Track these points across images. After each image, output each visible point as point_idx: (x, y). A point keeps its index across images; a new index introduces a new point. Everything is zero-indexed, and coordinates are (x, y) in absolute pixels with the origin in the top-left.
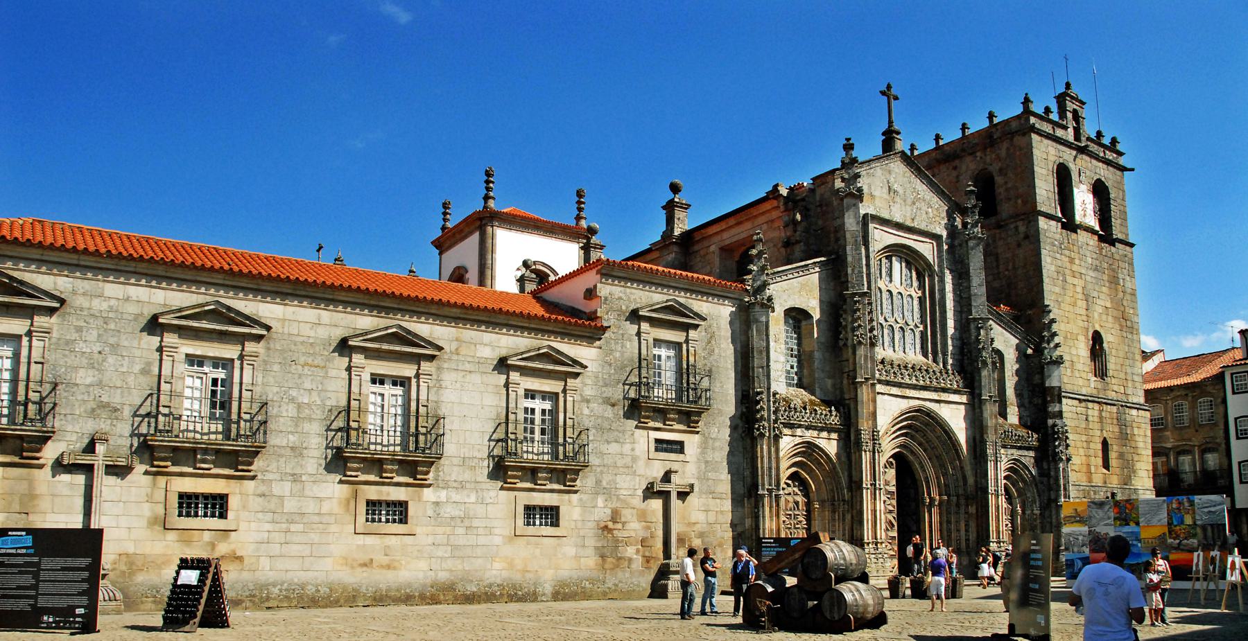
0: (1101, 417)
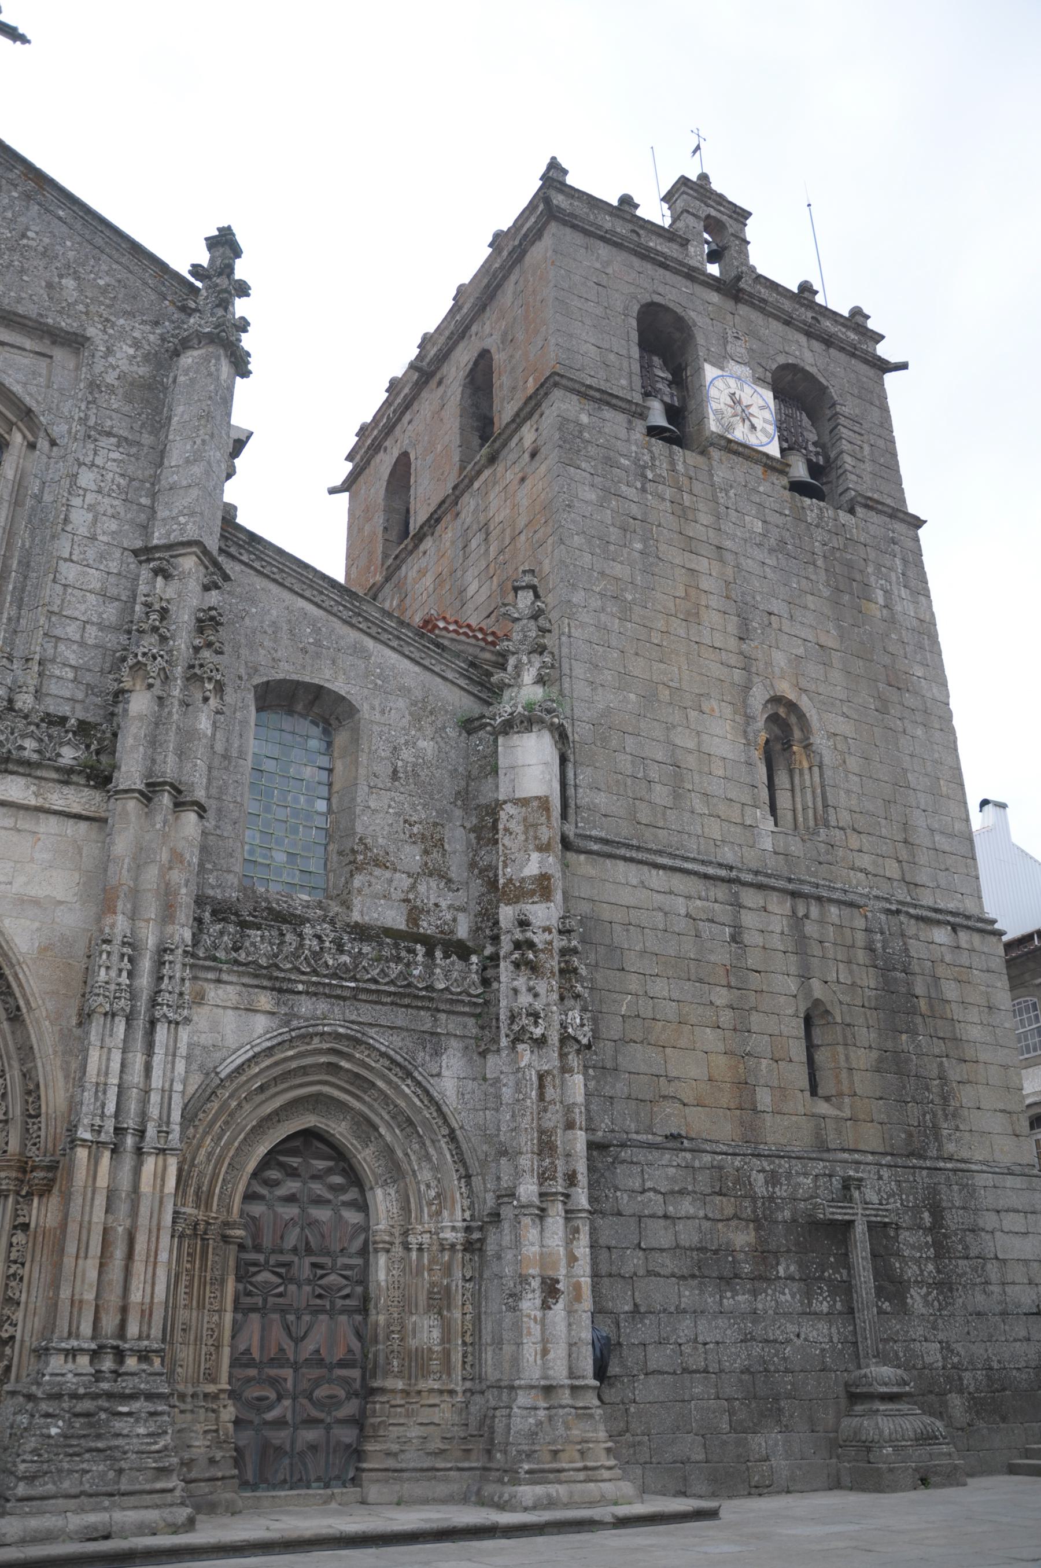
0: (801, 944)
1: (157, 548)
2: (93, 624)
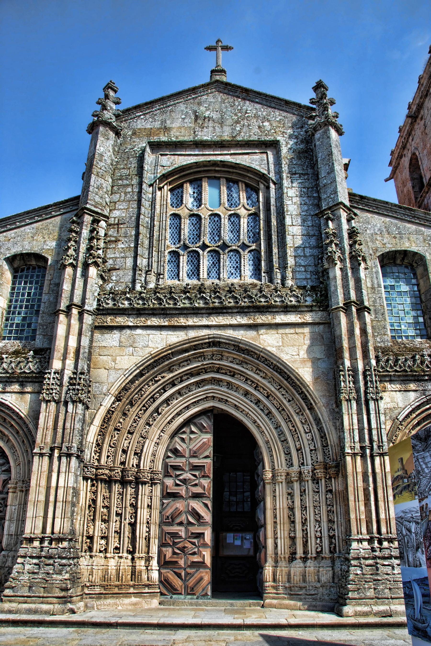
1: (325, 210)
2: (307, 247)
